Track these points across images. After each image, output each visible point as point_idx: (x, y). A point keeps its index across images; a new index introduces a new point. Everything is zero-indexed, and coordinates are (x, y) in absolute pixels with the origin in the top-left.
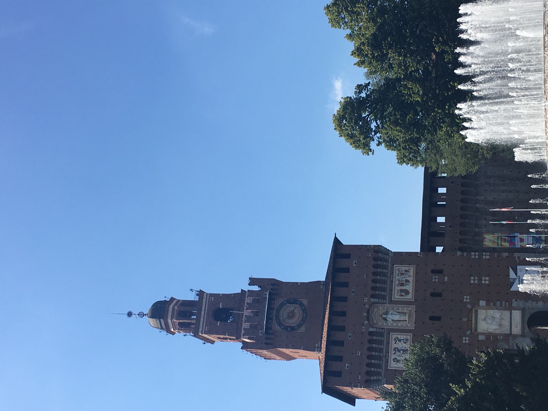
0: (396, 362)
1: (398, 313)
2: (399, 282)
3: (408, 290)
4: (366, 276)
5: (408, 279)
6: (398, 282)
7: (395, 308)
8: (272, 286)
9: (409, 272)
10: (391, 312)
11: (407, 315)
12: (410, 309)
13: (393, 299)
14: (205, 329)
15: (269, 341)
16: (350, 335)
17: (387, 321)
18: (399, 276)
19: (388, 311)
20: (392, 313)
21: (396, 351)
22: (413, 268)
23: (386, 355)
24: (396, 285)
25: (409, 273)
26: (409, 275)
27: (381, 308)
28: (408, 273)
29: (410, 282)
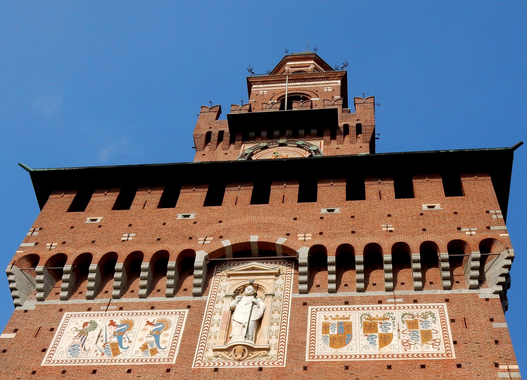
0: (81, 328)
1: (259, 322)
2: (381, 319)
3: (351, 344)
4: (391, 231)
5: (395, 341)
6: (381, 315)
7: (276, 316)
8: (354, 125)
9: (423, 342)
10: (262, 304)
11: (249, 342)
12: (273, 352)
13: (310, 308)
14: (262, 90)
15: (214, 138)
16: (192, 216)
17: (230, 299)
18: (403, 317)
19: (270, 299)
20: (259, 307)
21: (117, 326)
22: (443, 350)
23: (116, 304)
24: (366, 312)
25: (420, 342)
26: (411, 343)
27: (280, 281)
28: (420, 338)
29: (384, 348)
